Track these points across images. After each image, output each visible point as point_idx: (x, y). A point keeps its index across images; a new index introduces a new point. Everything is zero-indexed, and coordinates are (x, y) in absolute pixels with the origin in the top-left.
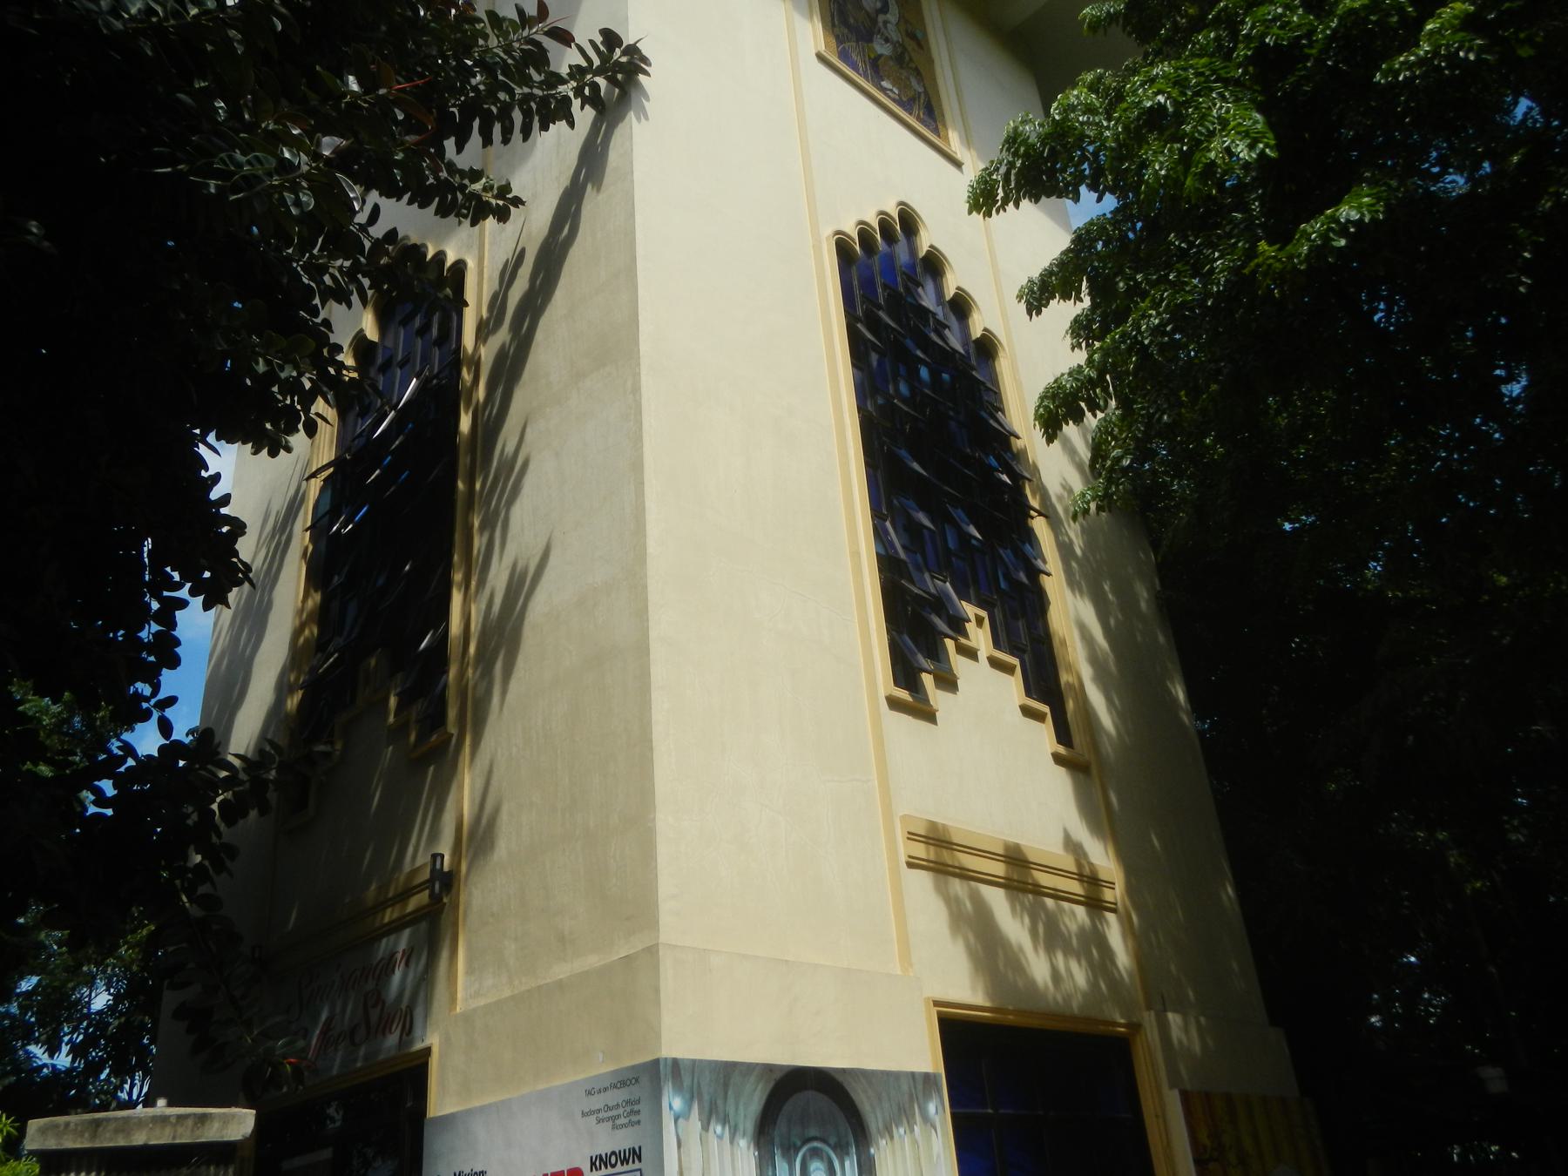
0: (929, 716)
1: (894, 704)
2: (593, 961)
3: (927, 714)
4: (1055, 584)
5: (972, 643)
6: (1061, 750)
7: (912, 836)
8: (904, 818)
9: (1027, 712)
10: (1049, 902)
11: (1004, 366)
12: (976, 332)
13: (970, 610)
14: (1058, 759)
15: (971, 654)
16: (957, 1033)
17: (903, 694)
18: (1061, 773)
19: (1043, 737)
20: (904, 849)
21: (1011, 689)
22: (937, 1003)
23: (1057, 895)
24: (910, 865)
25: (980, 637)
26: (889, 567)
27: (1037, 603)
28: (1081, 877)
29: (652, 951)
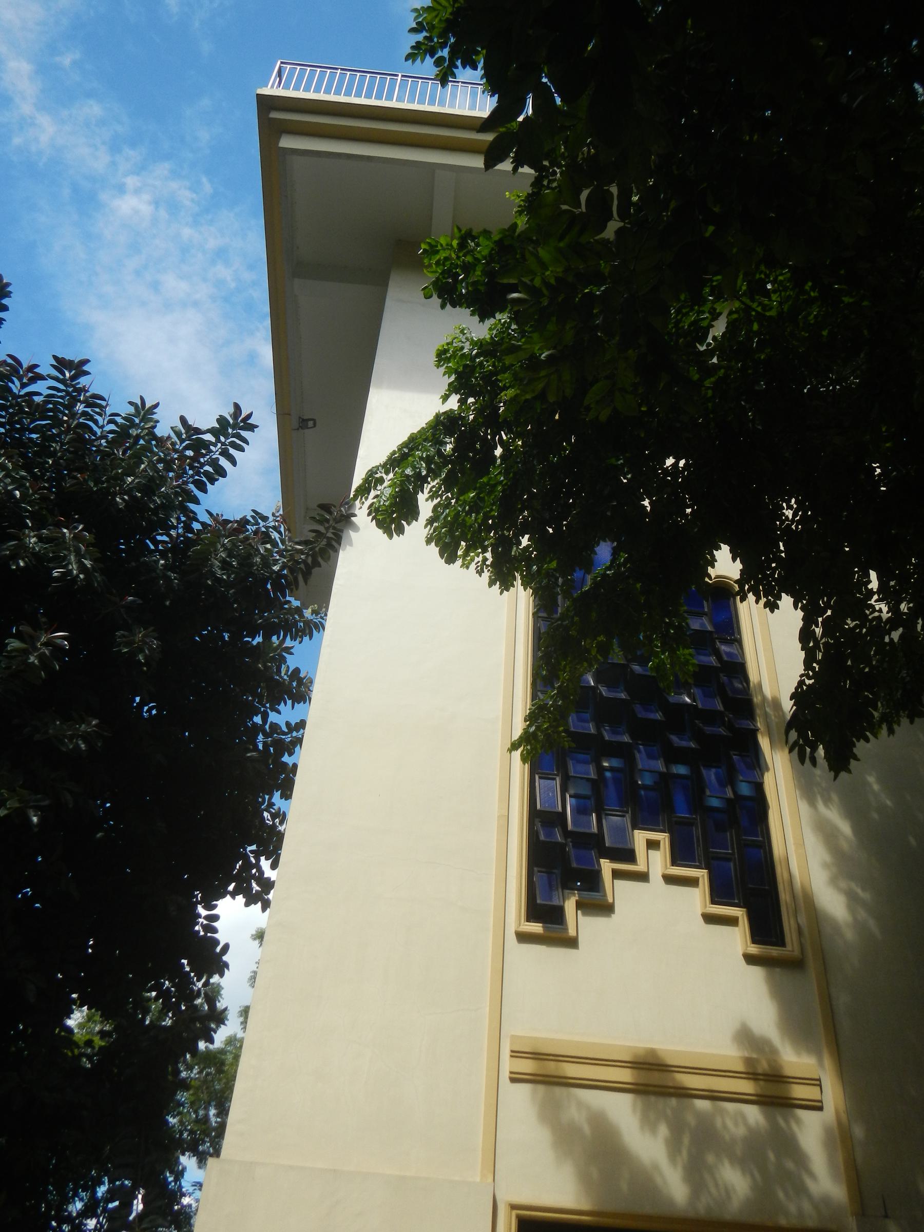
0: (572, 943)
1: (523, 937)
5: (640, 867)
6: (754, 949)
7: (516, 1054)
8: (514, 1038)
9: (710, 919)
10: (702, 1105)
13: (640, 838)
14: (750, 959)
15: (643, 877)
17: (536, 928)
18: (757, 974)
19: (736, 940)
20: (507, 1065)
21: (696, 899)
22: (513, 1207)
23: (713, 1096)
24: (513, 1080)
28: (752, 1075)
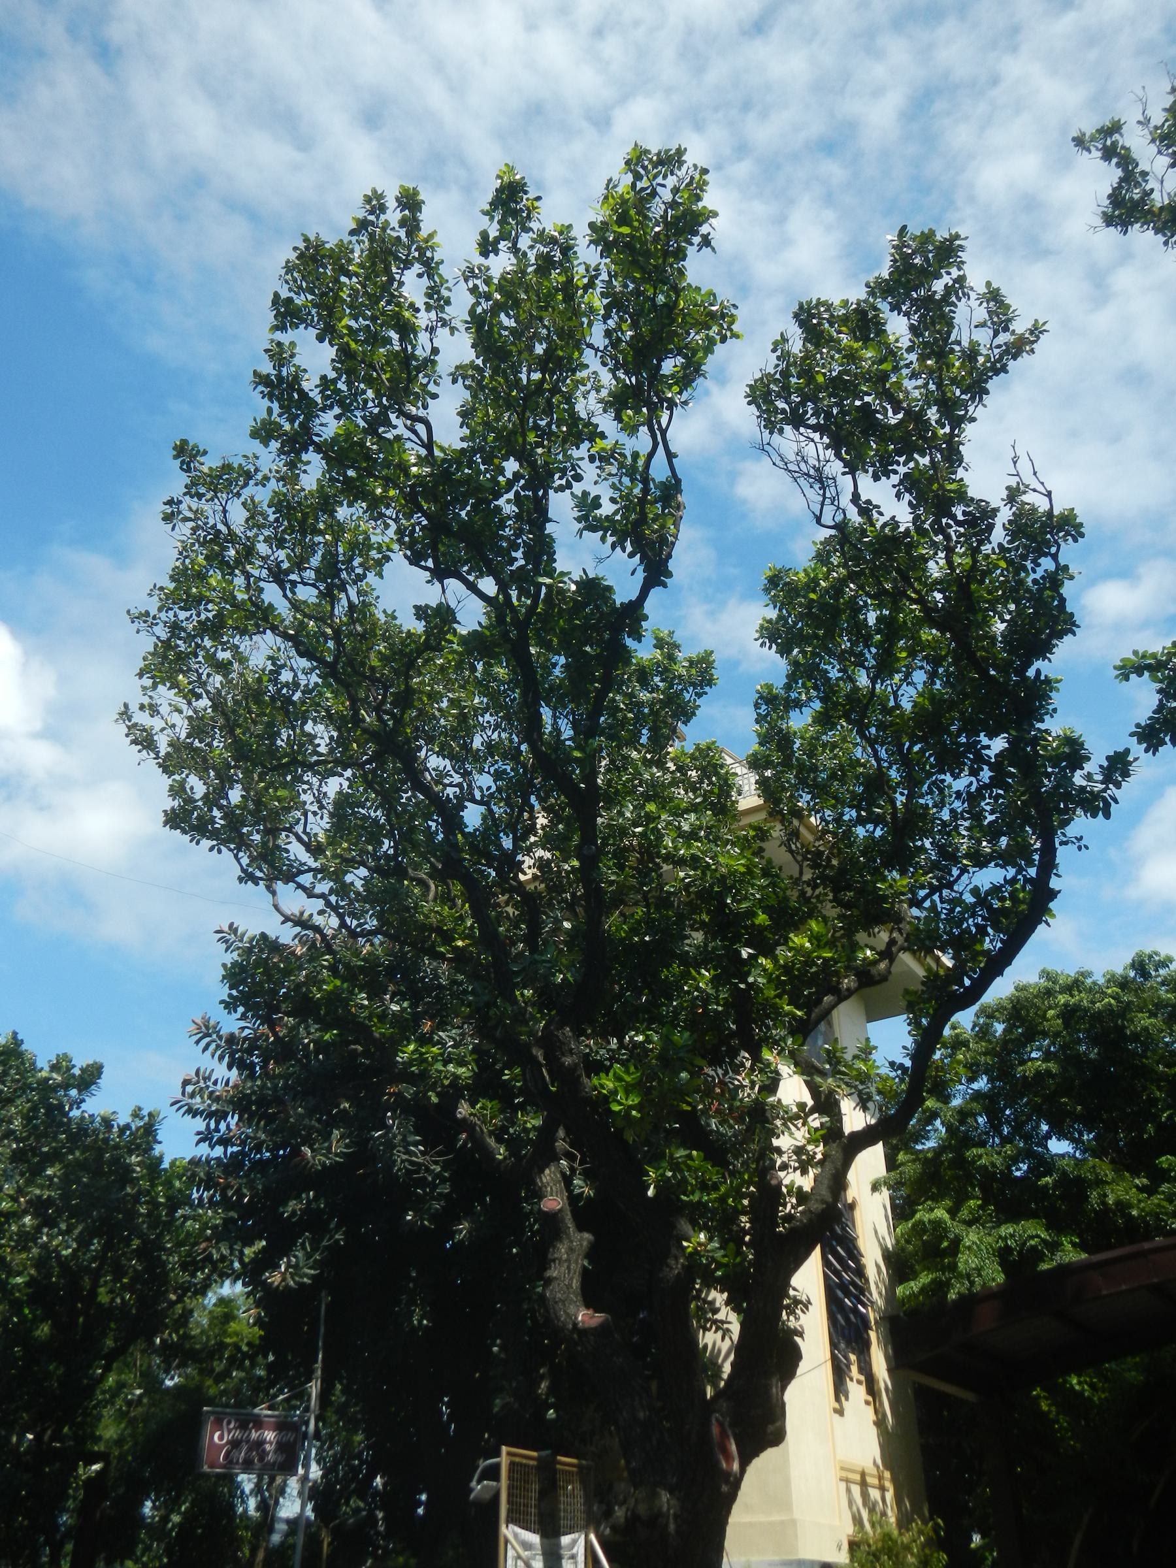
1: (835, 1411)
2: (762, 1518)
3: (840, 1412)
4: (873, 1335)
9: (867, 1403)
11: (858, 1214)
12: (850, 1201)
13: (853, 1357)
16: (853, 1546)
21: (862, 1389)
25: (854, 1369)
26: (833, 1345)
27: (867, 1344)
29: (793, 1522)
